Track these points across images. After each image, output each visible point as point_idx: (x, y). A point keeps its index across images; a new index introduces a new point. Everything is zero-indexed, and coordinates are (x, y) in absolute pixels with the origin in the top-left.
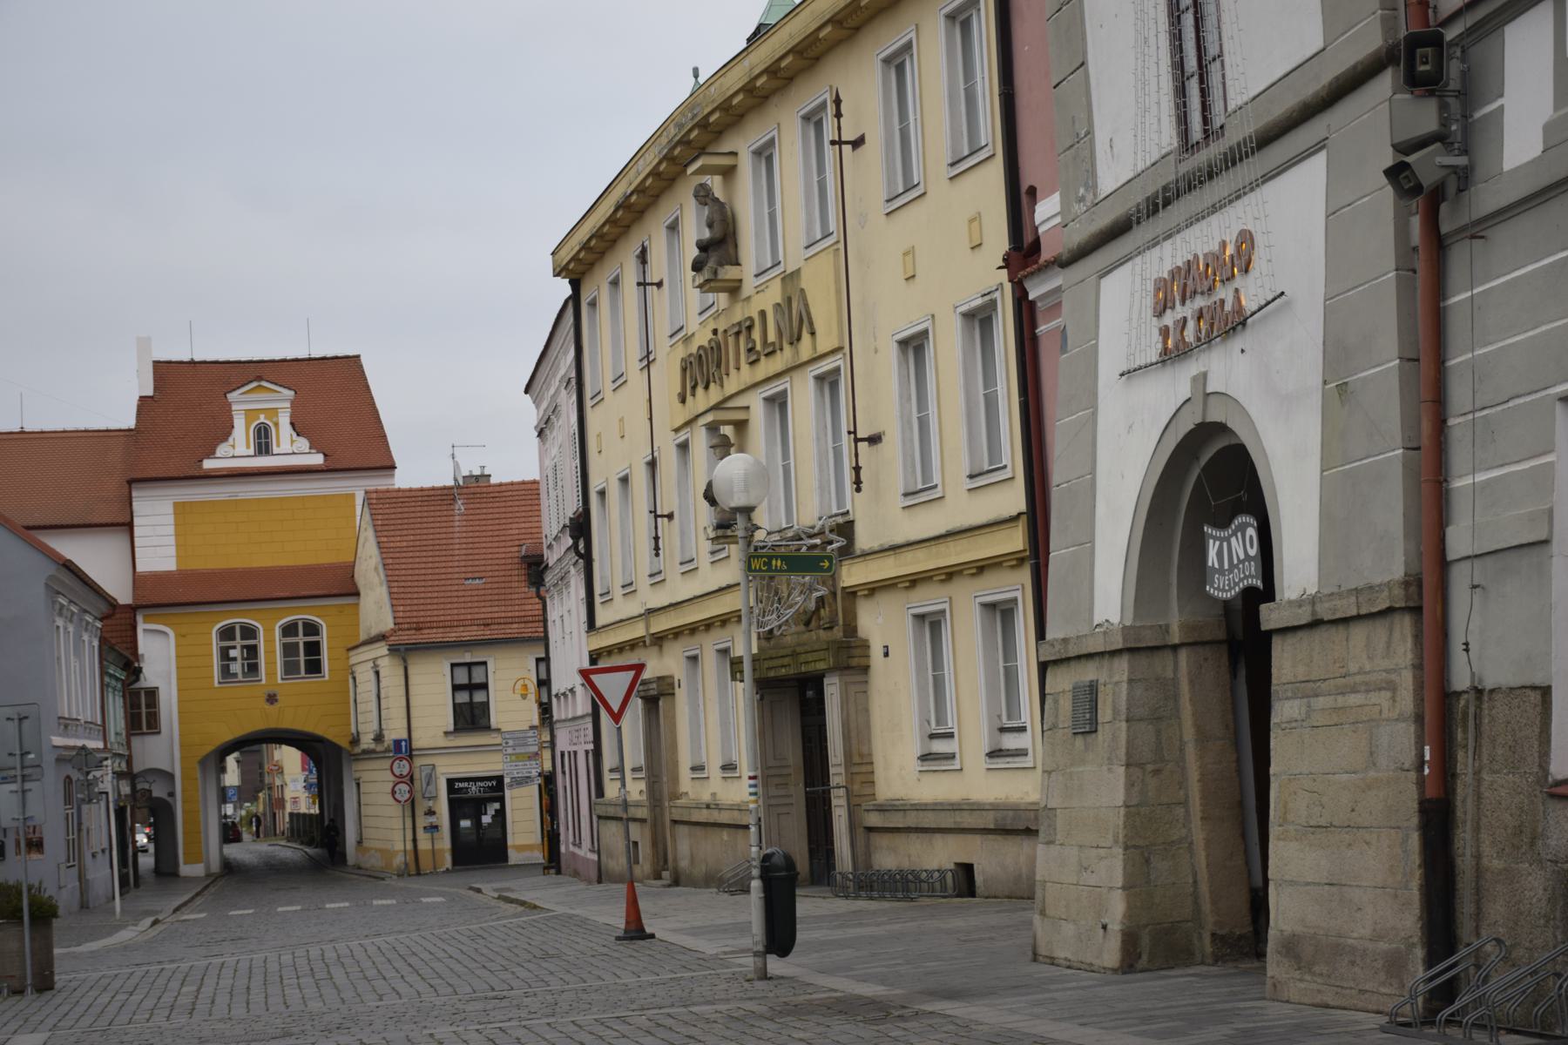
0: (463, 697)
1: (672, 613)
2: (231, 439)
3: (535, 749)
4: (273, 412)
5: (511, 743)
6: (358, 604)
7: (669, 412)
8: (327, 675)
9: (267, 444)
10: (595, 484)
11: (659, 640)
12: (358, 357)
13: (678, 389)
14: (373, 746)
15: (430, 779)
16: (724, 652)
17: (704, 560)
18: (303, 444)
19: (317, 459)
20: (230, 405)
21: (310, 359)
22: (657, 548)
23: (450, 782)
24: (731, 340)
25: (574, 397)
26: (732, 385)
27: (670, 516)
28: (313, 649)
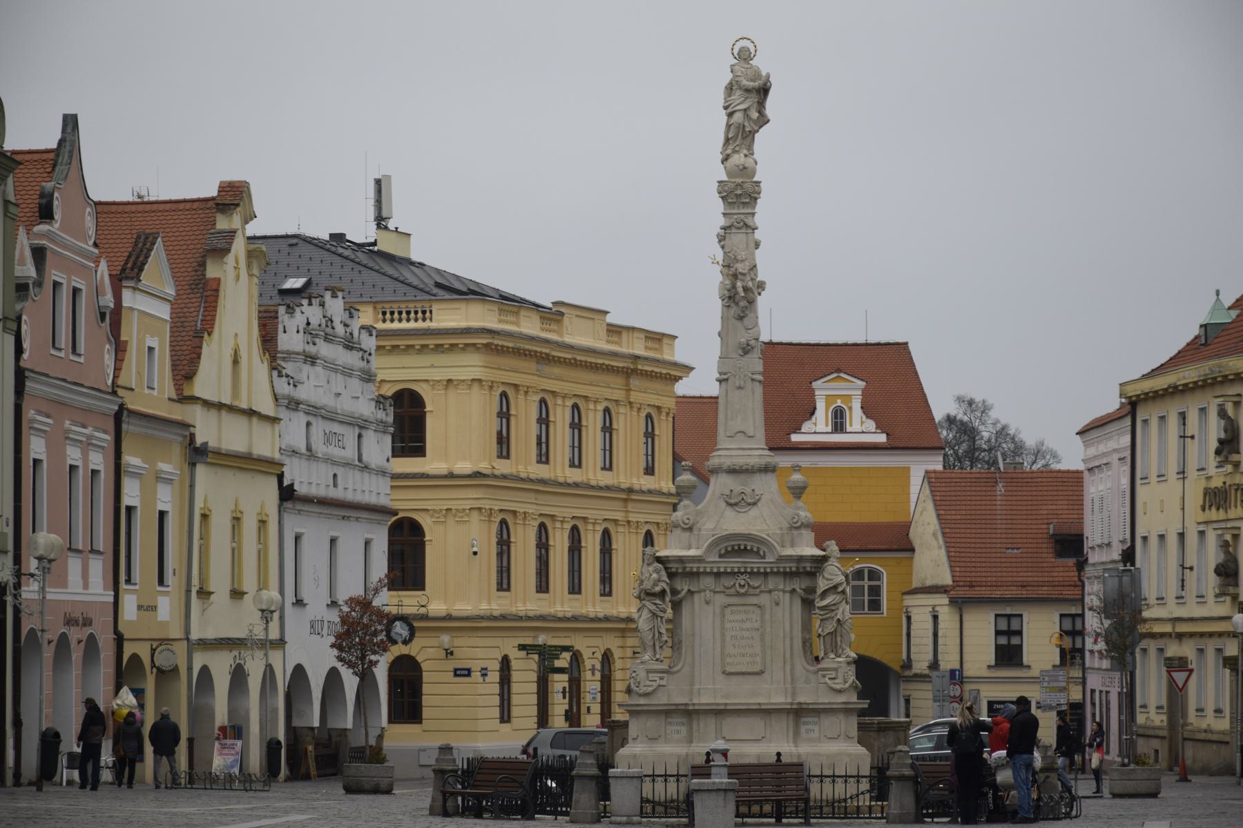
0: (1003, 640)
1: (1190, 624)
2: (814, 418)
3: (1064, 684)
4: (847, 398)
5: (1047, 679)
6: (912, 558)
7: (1194, 513)
8: (885, 612)
9: (842, 423)
10: (1140, 532)
11: (1180, 636)
12: (906, 344)
13: (1201, 503)
14: (927, 672)
15: (976, 699)
16: (1219, 651)
17: (1210, 598)
18: (871, 425)
19: (882, 438)
20: (813, 390)
21: (867, 344)
22: (1183, 586)
23: (990, 704)
24: (1233, 492)
25: (1127, 468)
26: (1232, 513)
27: (1191, 569)
28: (875, 591)
